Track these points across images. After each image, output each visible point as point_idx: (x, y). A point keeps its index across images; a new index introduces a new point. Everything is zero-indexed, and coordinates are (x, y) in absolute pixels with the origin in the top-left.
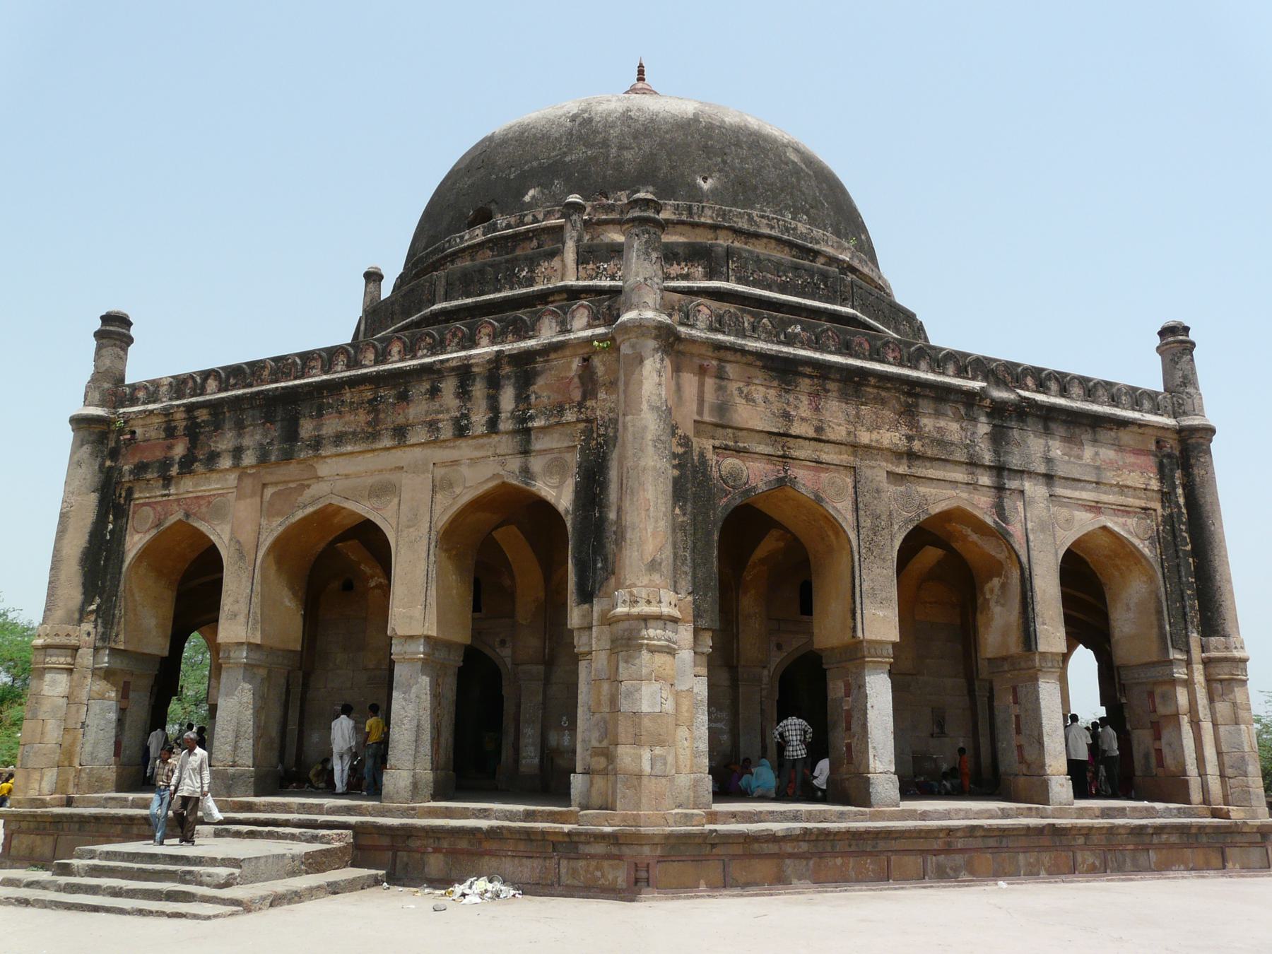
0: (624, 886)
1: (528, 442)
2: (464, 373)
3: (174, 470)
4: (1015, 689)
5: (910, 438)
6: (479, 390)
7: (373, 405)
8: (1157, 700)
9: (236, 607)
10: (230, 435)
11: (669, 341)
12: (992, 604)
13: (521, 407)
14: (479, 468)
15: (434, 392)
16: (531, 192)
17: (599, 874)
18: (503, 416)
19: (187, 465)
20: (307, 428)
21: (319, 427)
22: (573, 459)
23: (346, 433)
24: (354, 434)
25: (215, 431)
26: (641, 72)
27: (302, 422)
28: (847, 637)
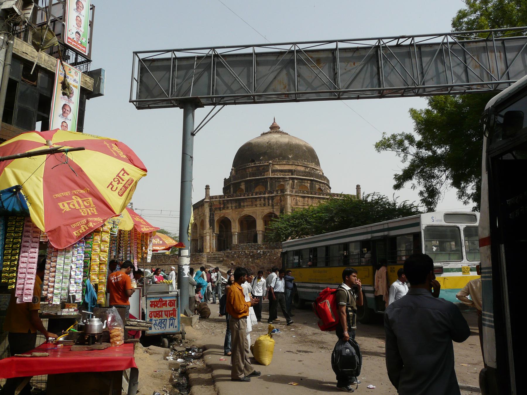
2: (264, 198)
6: (266, 200)
11: (291, 195)
14: (267, 210)
15: (260, 200)
19: (224, 208)
20: (242, 204)
22: (279, 209)
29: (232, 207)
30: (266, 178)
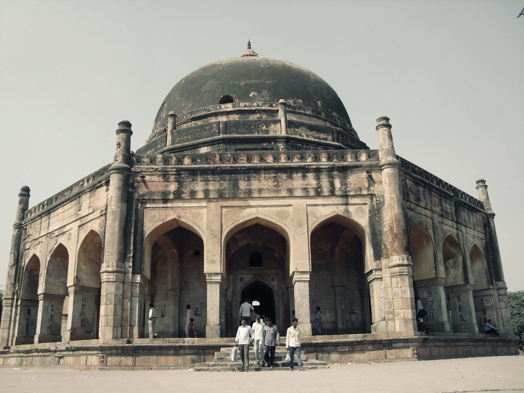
0: (410, 357)
1: (347, 200)
2: (318, 171)
3: (171, 197)
4: (458, 297)
5: (442, 210)
7: (275, 179)
8: (484, 302)
9: (214, 258)
10: (201, 184)
12: (449, 268)
13: (344, 187)
15: (304, 177)
16: (252, 93)
17: (400, 353)
18: (337, 189)
19: (178, 196)
20: (243, 185)
21: (250, 185)
23: (263, 189)
24: (268, 189)
25: (193, 181)
26: (249, 45)
27: (240, 182)
28: (433, 276)
29: (206, 192)
30: (275, 139)
